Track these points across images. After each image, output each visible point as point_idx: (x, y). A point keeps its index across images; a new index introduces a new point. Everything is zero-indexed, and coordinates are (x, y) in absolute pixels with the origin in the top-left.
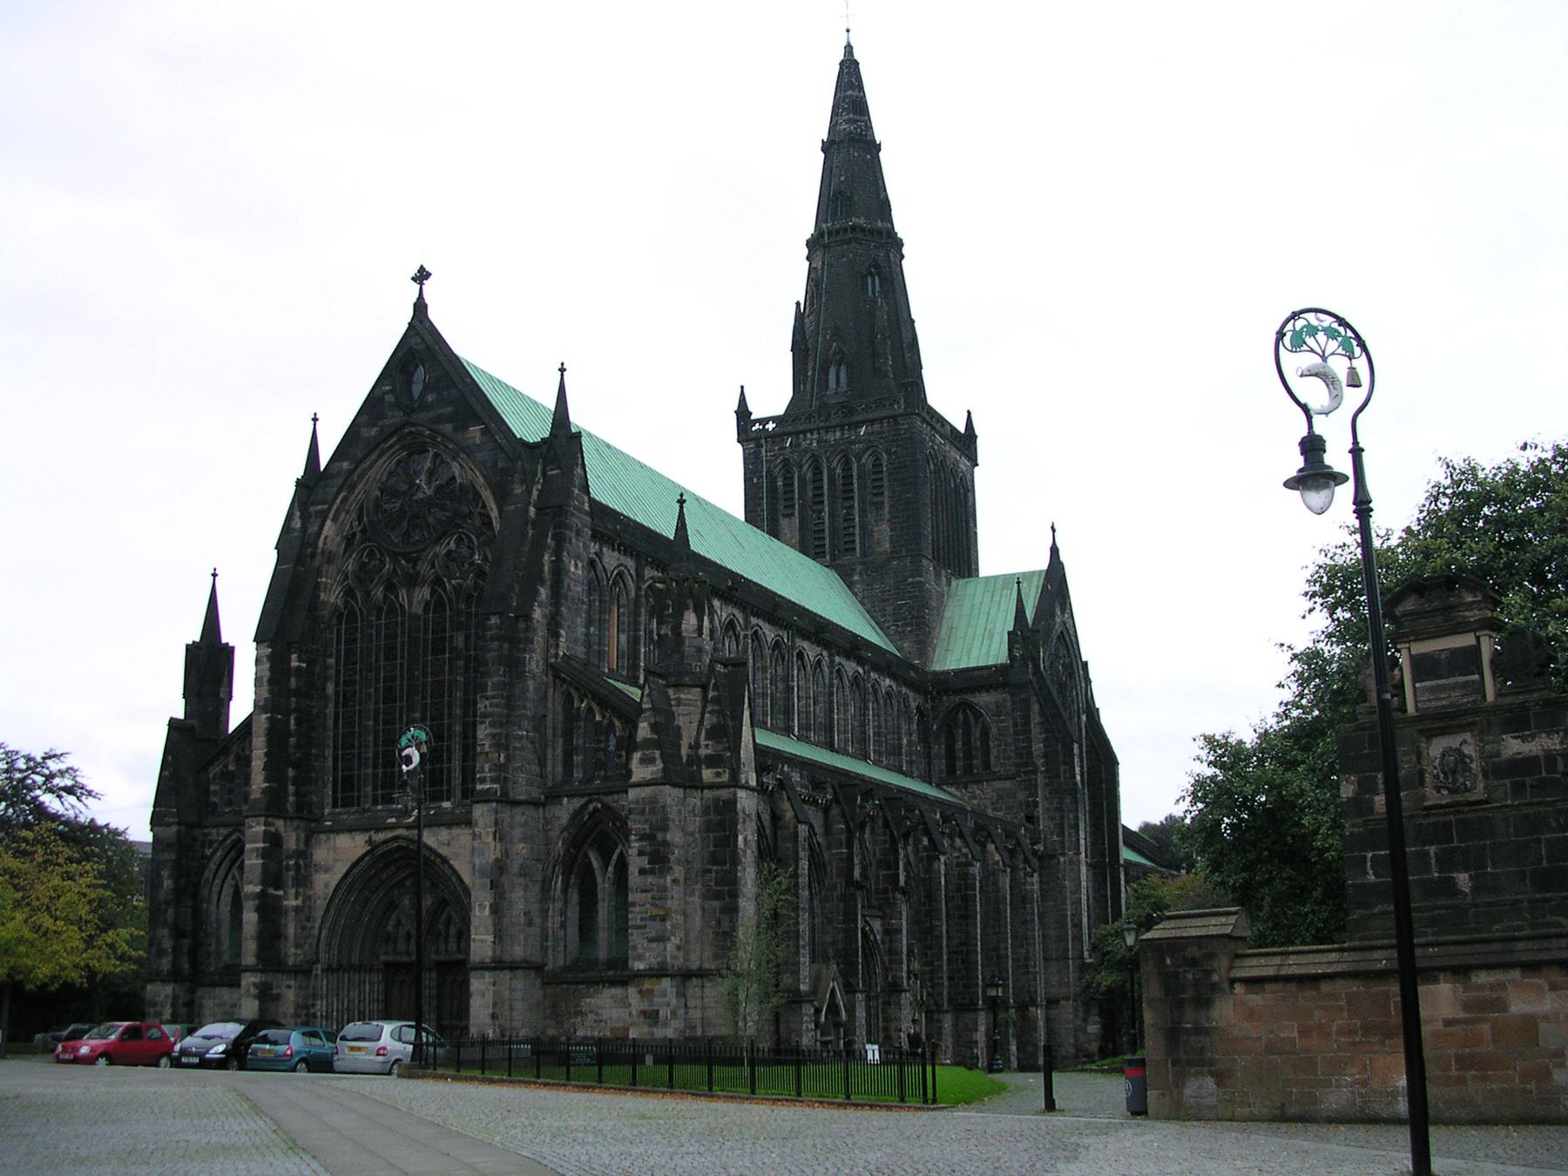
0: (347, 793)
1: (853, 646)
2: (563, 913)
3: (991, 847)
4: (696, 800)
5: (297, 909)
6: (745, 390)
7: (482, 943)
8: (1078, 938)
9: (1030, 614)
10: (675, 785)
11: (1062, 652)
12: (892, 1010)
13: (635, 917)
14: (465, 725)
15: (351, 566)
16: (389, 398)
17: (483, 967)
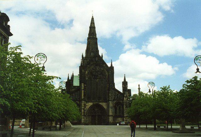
17: (111, 116)
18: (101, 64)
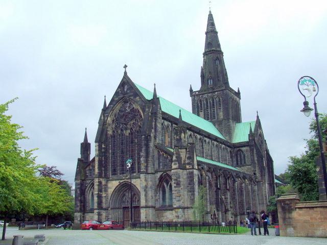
0: (114, 172)
1: (216, 139)
2: (159, 196)
3: (246, 180)
4: (185, 172)
5: (105, 197)
7: (143, 203)
8: (266, 199)
9: (253, 130)
10: (181, 169)
11: (260, 138)
12: (227, 215)
13: (174, 196)
14: (138, 158)
15: (114, 126)
16: (120, 92)
17: (143, 207)
18: (132, 98)
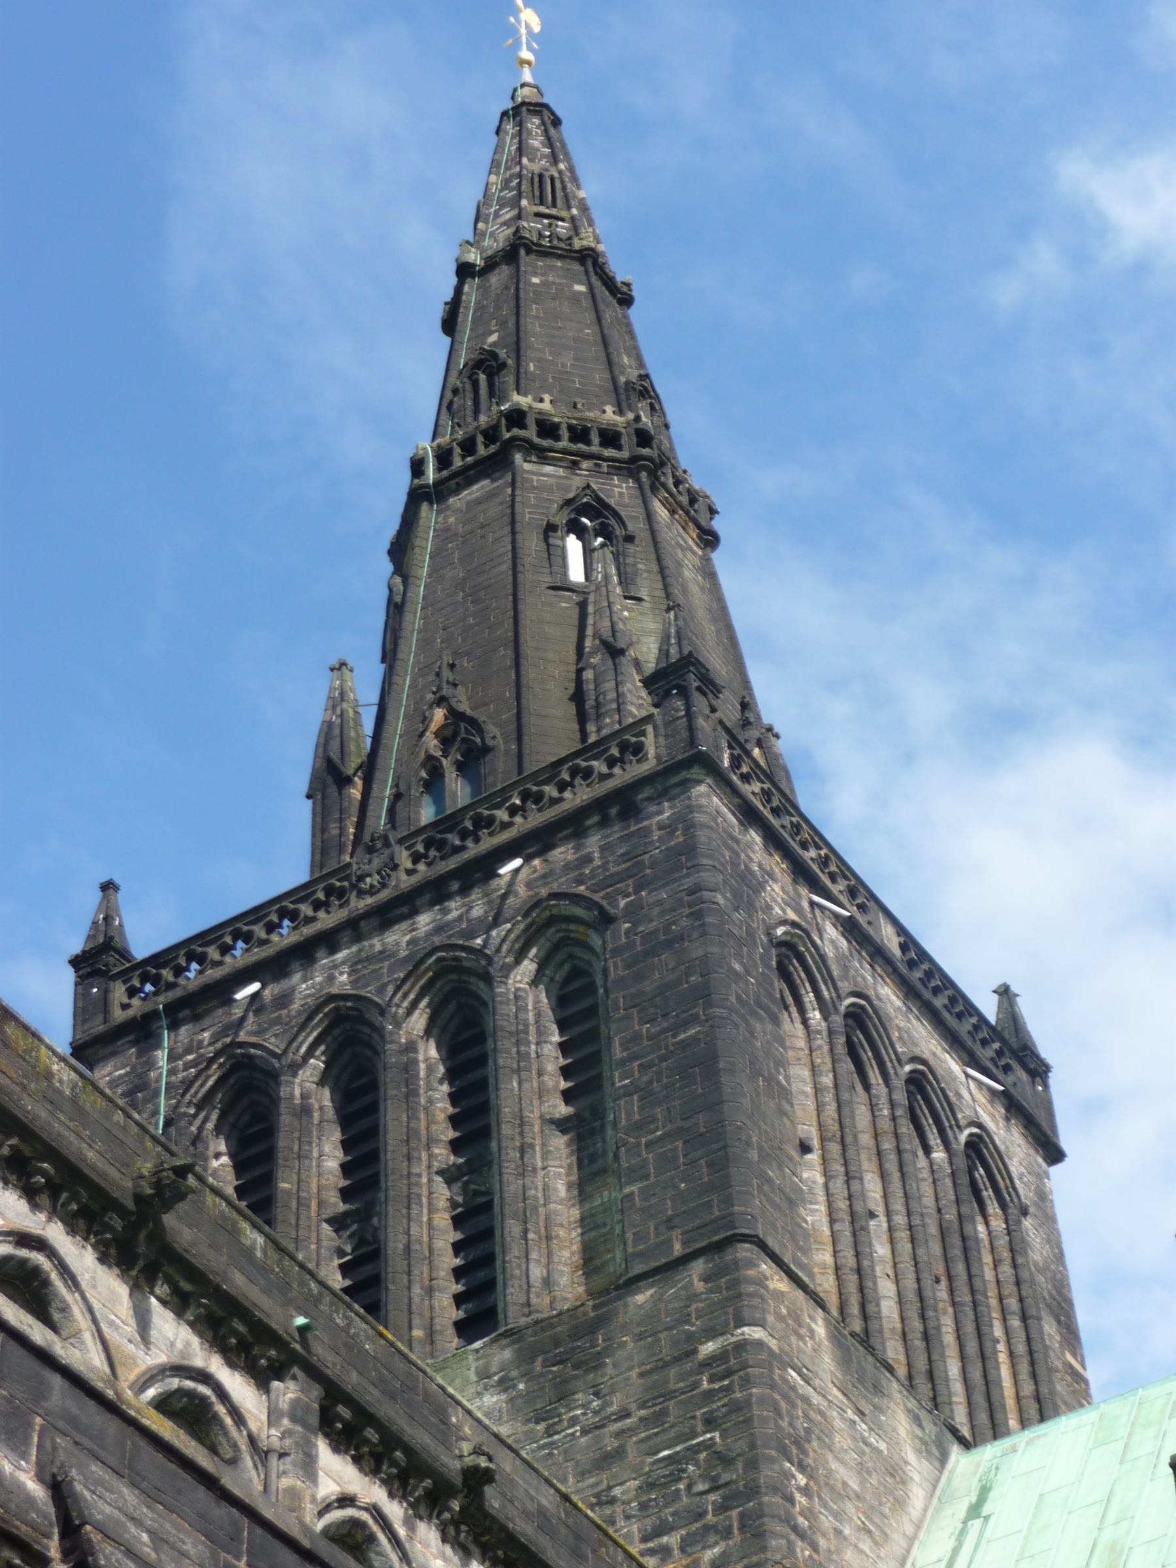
6: (121, 897)
